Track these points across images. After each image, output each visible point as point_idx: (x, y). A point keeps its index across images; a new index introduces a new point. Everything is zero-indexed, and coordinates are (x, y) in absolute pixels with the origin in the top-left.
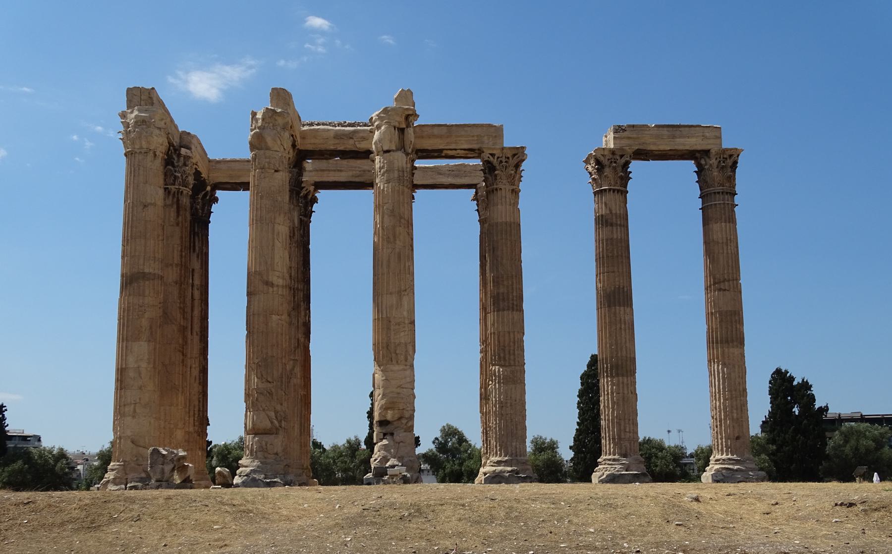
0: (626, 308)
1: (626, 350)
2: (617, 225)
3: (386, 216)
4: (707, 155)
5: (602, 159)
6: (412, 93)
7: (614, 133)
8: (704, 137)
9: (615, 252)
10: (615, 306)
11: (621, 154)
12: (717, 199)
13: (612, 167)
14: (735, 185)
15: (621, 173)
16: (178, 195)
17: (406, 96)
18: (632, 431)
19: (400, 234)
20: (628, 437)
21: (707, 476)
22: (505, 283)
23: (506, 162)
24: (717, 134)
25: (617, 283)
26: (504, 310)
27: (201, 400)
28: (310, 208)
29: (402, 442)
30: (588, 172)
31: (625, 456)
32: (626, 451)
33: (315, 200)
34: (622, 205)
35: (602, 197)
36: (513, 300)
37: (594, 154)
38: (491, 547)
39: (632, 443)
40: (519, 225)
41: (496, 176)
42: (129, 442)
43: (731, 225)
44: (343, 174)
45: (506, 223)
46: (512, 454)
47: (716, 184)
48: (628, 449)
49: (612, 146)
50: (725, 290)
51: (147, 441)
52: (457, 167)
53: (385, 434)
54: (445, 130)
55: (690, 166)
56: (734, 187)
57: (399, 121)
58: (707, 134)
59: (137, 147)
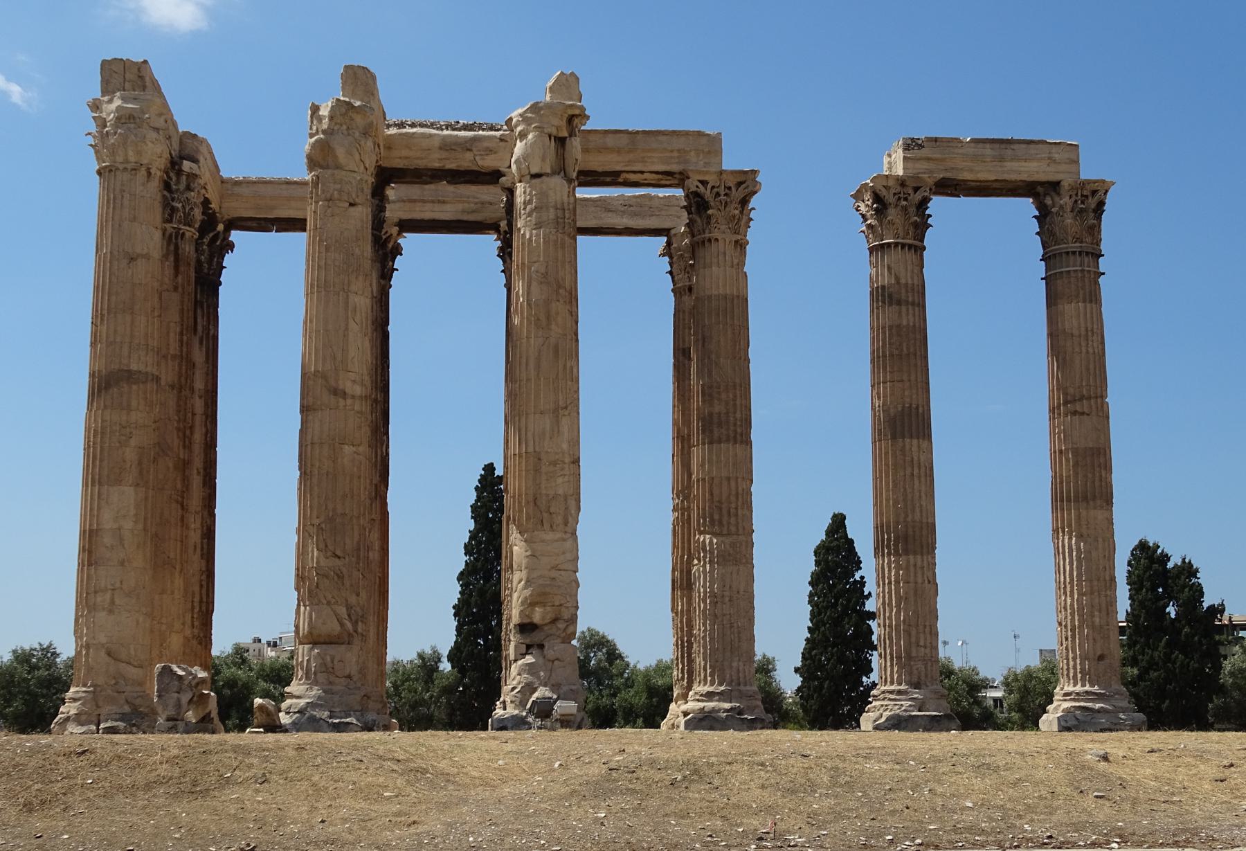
0: (921, 441)
1: (921, 511)
2: (907, 303)
5: (883, 192)
6: (578, 79)
7: (905, 150)
8: (1052, 160)
9: (905, 349)
10: (903, 437)
11: (915, 185)
12: (1071, 263)
13: (899, 208)
14: (1101, 240)
15: (916, 218)
16: (176, 238)
17: (567, 83)
18: (928, 645)
19: (557, 313)
20: (923, 655)
21: (1049, 720)
22: (724, 396)
23: (725, 195)
24: (1073, 157)
25: (908, 400)
26: (720, 441)
27: (204, 583)
28: (391, 263)
29: (557, 659)
30: (861, 214)
31: (917, 686)
32: (919, 678)
33: (397, 251)
34: (918, 268)
35: (883, 257)
36: (735, 425)
37: (871, 185)
38: (825, 830)
39: (930, 664)
40: (747, 299)
41: (709, 217)
42: (103, 654)
43: (1094, 306)
44: (448, 207)
45: (725, 297)
46: (732, 681)
47: (1070, 239)
48: (923, 674)
49: (900, 172)
50: (1083, 414)
51: (132, 652)
52: (639, 200)
53: (529, 647)
54: (624, 140)
55: (1027, 206)
56: (1098, 242)
57: (557, 125)
58: (1056, 156)
59: (120, 159)
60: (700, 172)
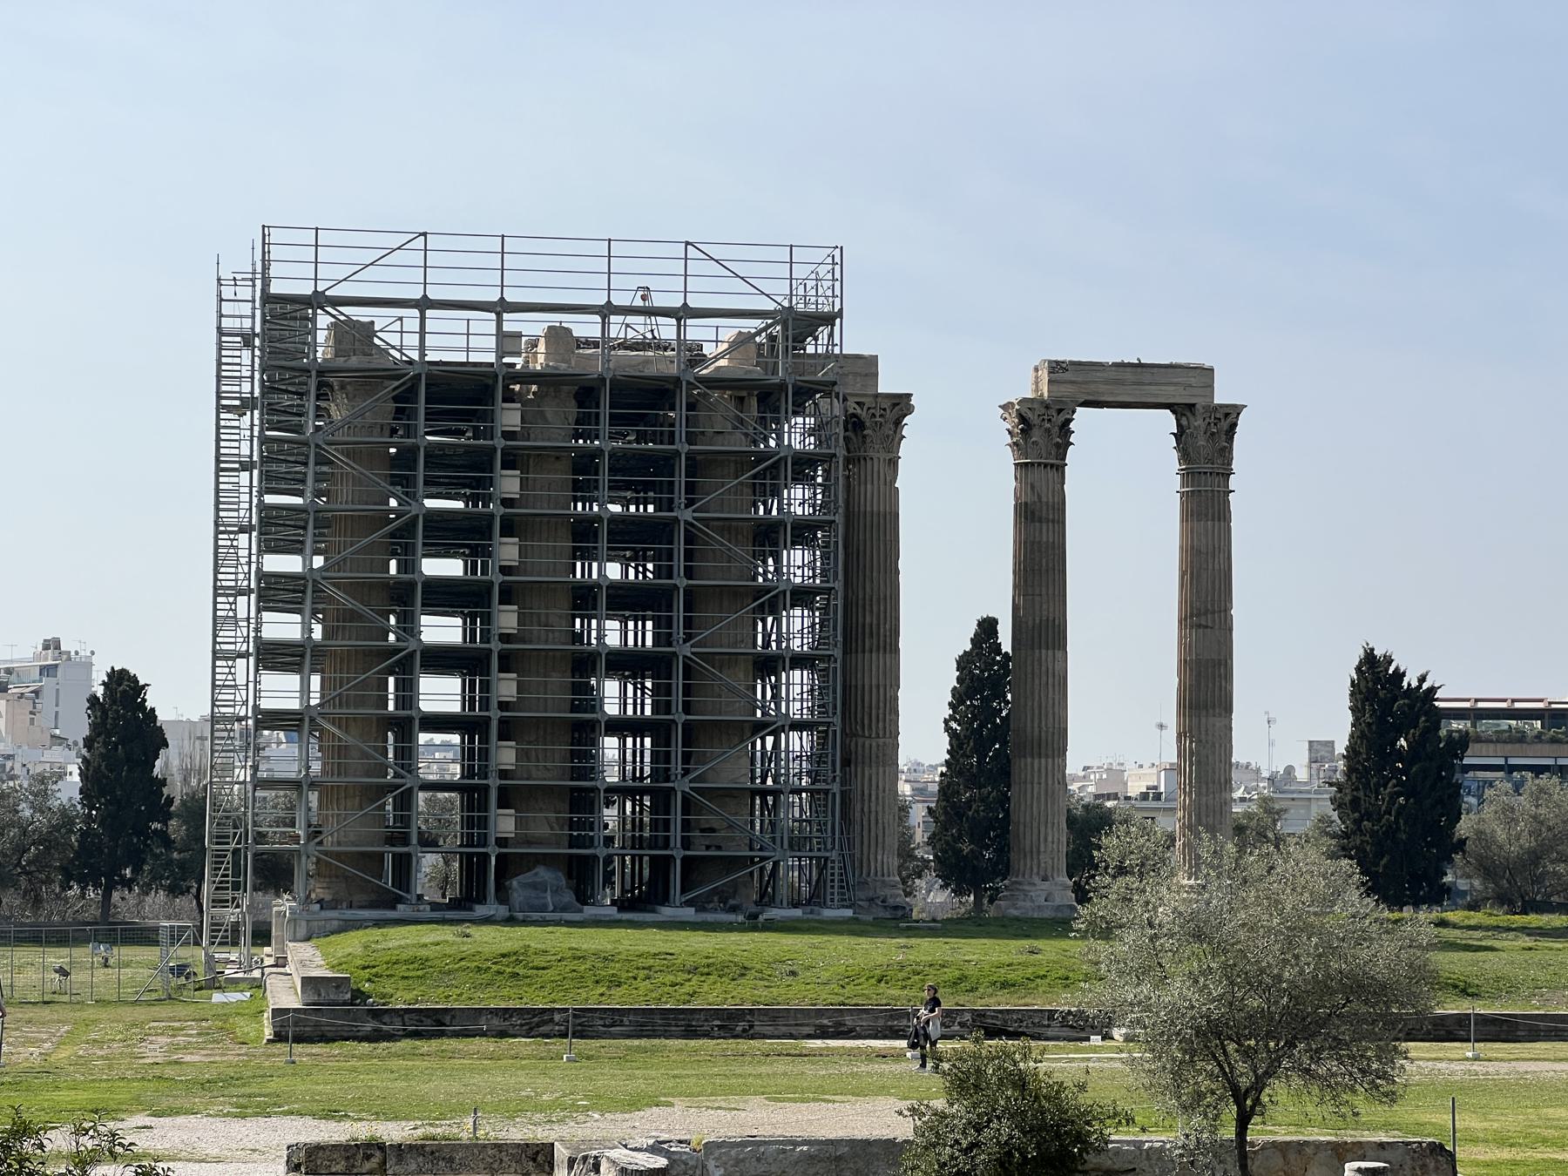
5: (1029, 415)
7: (1050, 373)
9: (1044, 564)
15: (1058, 440)
23: (881, 416)
41: (864, 437)
50: (1207, 627)
60: (856, 395)
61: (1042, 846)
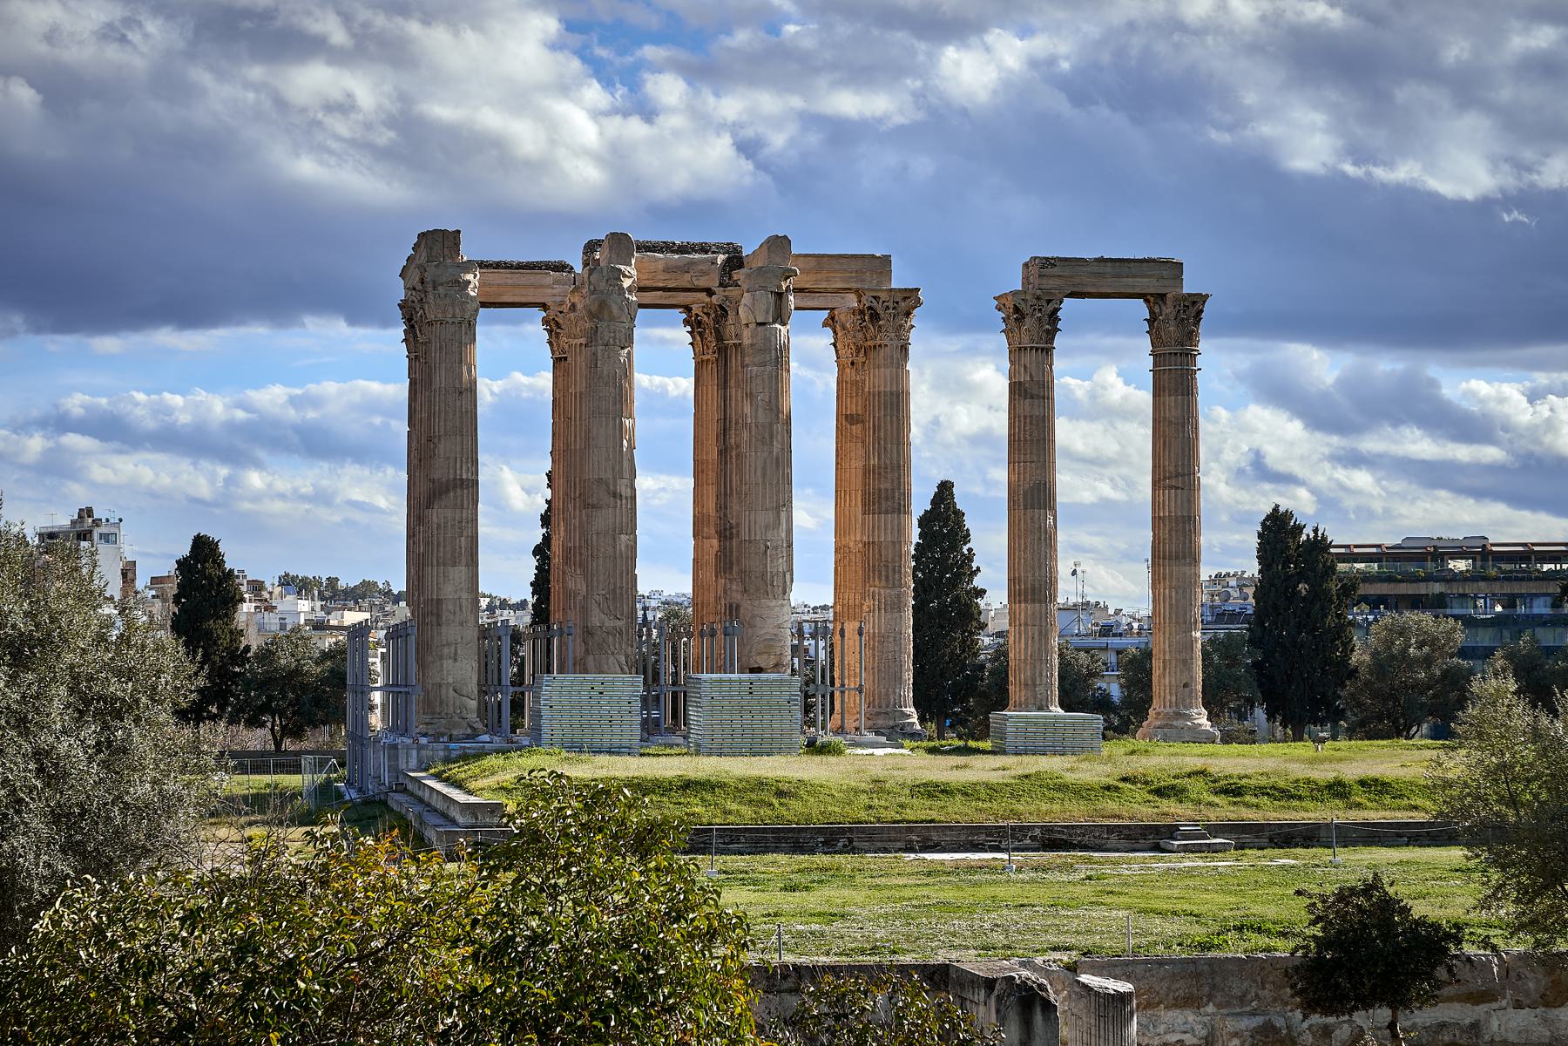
3: (760, 411)
4: (1162, 300)
5: (1022, 306)
23: (894, 308)
26: (887, 512)
41: (880, 327)
50: (1177, 488)
61: (1038, 679)
